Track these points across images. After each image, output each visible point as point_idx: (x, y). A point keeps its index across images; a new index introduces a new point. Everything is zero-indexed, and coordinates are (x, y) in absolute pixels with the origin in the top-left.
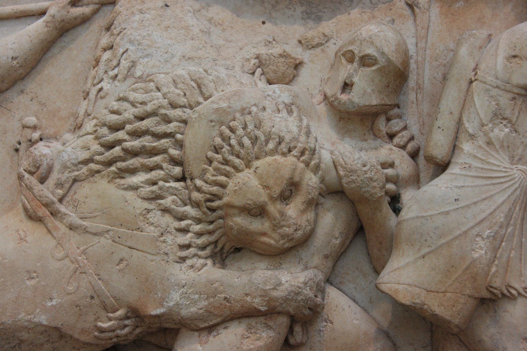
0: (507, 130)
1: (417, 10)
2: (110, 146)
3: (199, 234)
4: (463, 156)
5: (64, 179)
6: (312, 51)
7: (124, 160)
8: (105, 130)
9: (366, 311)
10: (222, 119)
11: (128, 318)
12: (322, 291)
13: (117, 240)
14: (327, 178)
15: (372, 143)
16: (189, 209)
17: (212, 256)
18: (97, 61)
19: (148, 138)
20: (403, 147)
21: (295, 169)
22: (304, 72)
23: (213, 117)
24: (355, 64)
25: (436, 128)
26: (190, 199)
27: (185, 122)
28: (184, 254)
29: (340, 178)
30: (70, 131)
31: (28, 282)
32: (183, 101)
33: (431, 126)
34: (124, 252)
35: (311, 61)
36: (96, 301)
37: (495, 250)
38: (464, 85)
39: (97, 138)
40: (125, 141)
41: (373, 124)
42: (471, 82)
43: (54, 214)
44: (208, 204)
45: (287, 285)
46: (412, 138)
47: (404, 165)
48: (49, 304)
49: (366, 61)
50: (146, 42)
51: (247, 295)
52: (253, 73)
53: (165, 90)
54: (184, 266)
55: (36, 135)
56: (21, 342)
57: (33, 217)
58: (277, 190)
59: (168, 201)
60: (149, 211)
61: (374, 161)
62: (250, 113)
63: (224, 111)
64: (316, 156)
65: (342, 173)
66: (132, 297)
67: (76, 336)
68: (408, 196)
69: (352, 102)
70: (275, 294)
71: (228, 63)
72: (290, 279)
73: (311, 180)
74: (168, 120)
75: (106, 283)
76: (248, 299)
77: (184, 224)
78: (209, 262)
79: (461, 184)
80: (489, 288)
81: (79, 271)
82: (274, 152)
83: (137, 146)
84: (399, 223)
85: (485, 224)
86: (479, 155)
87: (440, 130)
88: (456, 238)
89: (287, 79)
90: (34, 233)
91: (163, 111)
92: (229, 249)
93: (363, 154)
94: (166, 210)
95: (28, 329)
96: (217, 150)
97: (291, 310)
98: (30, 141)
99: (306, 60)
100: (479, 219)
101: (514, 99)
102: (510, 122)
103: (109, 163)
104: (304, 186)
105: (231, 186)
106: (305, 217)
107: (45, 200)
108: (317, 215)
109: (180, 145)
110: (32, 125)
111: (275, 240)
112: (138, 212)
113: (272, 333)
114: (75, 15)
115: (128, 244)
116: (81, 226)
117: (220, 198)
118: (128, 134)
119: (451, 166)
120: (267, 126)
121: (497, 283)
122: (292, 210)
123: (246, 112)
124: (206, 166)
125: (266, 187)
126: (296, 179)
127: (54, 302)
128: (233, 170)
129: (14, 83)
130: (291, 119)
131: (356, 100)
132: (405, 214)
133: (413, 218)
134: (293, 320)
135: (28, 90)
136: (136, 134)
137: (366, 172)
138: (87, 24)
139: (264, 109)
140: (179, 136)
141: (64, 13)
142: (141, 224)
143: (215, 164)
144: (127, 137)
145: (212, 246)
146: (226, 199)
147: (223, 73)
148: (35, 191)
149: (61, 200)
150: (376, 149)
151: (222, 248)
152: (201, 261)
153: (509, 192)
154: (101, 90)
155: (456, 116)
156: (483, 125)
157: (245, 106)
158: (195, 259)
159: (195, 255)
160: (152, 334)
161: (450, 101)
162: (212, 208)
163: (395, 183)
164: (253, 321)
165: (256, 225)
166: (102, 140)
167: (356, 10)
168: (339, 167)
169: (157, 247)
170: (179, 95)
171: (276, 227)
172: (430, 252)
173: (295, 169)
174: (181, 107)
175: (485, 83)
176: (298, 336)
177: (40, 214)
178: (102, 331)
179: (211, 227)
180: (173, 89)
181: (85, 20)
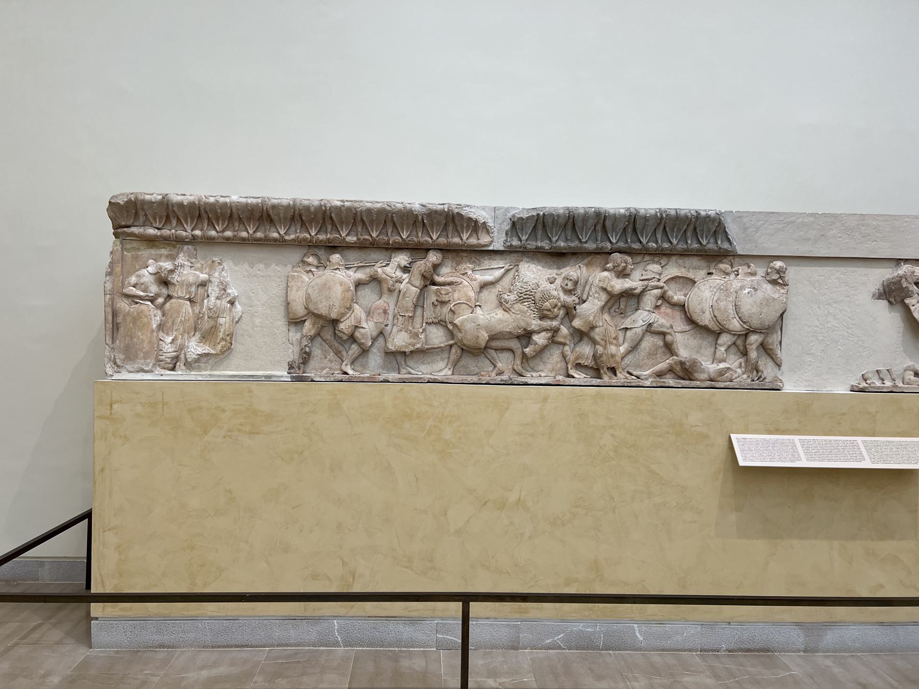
47: (577, 301)
72: (555, 323)
92: (542, 317)
161: (587, 288)
162: (540, 310)
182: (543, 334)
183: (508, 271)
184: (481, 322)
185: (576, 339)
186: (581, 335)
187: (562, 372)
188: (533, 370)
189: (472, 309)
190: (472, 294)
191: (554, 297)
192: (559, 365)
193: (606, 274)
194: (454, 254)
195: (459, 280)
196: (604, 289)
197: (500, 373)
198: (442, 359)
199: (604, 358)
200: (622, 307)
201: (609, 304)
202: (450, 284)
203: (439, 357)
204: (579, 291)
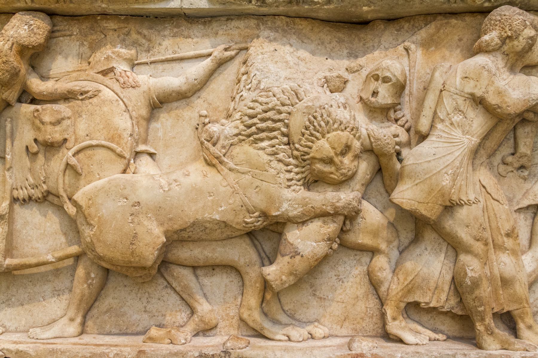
0: (461, 117)
1: (410, 52)
2: (249, 127)
3: (297, 173)
4: (437, 131)
5: (226, 144)
6: (353, 74)
7: (257, 134)
8: (246, 118)
9: (382, 212)
10: (309, 110)
11: (260, 217)
12: (360, 202)
13: (255, 176)
14: (364, 143)
15: (387, 124)
16: (291, 160)
17: (303, 185)
18: (239, 81)
19: (270, 122)
20: (403, 126)
21: (348, 139)
22: (349, 85)
23: (305, 111)
24: (380, 82)
25: (422, 115)
26: (292, 154)
27: (289, 113)
28: (289, 183)
29: (371, 143)
30: (224, 118)
31: (209, 198)
32: (288, 102)
33: (420, 114)
34: (258, 183)
35: (353, 80)
36: (244, 208)
37: (454, 180)
38: (438, 93)
39: (242, 122)
40: (258, 123)
41: (387, 114)
42: (441, 91)
43: (221, 162)
44: (302, 157)
45: (344, 200)
46: (407, 121)
47: (403, 137)
48: (220, 209)
49: (386, 80)
50: (265, 70)
51: (323, 205)
52: (323, 87)
53: (278, 96)
54: (290, 190)
55: (207, 120)
56: (206, 228)
57: (209, 164)
58: (339, 150)
59: (281, 156)
60: (271, 161)
61: (389, 134)
62: (324, 108)
63: (311, 107)
64: (359, 131)
65: (372, 140)
66: (263, 206)
67: (234, 226)
68: (405, 152)
69: (378, 102)
70: (338, 204)
71: (310, 81)
72: (346, 197)
73: (357, 145)
74: (280, 113)
75: (249, 199)
76: (324, 207)
77: (289, 168)
78: (302, 188)
79: (437, 146)
80: (450, 200)
81: (235, 192)
82: (336, 130)
83: (263, 126)
84: (402, 167)
85: (449, 167)
86: (446, 131)
87: (424, 117)
88: (434, 174)
89: (340, 90)
90: (211, 172)
91: (277, 108)
92: (313, 181)
93: (383, 130)
94: (280, 161)
95: (209, 222)
96: (307, 128)
97: (346, 213)
98: (204, 123)
99: (350, 79)
100: (446, 164)
101: (465, 100)
102: (463, 112)
103: (249, 136)
104: (353, 148)
105: (314, 147)
106: (353, 164)
107: (216, 155)
108: (359, 162)
109: (287, 126)
110: (204, 115)
111: (337, 176)
112: (265, 161)
113: (335, 225)
114: (226, 56)
115: (261, 178)
116: (235, 169)
117: (308, 154)
118: (259, 120)
119: (429, 137)
120: (334, 115)
121: (455, 198)
122: (347, 160)
123: (322, 108)
124: (301, 137)
125: (334, 148)
126: (349, 144)
127: (223, 209)
128: (315, 139)
129: (194, 93)
130: (346, 111)
131: (380, 101)
132: (406, 162)
133: (410, 164)
134: (346, 217)
135: (202, 96)
136: (263, 120)
137: (385, 140)
138: (233, 61)
139: (332, 106)
140: (286, 121)
141: (221, 54)
142: (267, 168)
143: (306, 136)
144: (258, 122)
145: (303, 179)
146: (311, 155)
147: (308, 87)
148: (211, 151)
149: (224, 155)
150: (389, 127)
151: (308, 180)
152: (298, 187)
153: (462, 150)
154: (242, 96)
155: (433, 110)
156: (448, 114)
157: (321, 104)
158: (295, 186)
159: (296, 184)
160: (272, 225)
162: (304, 160)
163: (399, 145)
164: (326, 219)
165: (327, 169)
166: (245, 123)
167: (377, 52)
168: (371, 138)
169: (276, 180)
170: (286, 99)
171: (338, 169)
172: (420, 182)
173: (348, 139)
174: (287, 105)
175: (450, 92)
176: (348, 227)
177: (214, 163)
178: (247, 223)
179: (303, 169)
180: (282, 95)
181: (232, 58)
182: (315, 226)
183: (221, 64)
184: (143, 196)
185: (406, 236)
186: (418, 227)
187: (371, 324)
188: (295, 319)
189: (129, 160)
190: (124, 123)
191: (342, 126)
192: (361, 306)
193: (481, 60)
194: (85, 26)
195: (89, 86)
196: (479, 102)
197: (206, 330)
198: (57, 293)
199: (485, 290)
200: (523, 149)
201: (491, 144)
202: (67, 97)
203: (47, 288)
204: (406, 112)
